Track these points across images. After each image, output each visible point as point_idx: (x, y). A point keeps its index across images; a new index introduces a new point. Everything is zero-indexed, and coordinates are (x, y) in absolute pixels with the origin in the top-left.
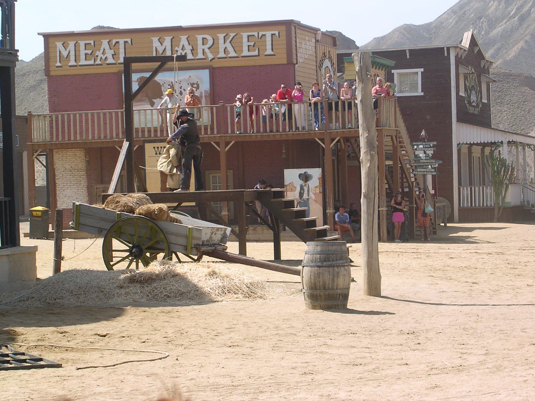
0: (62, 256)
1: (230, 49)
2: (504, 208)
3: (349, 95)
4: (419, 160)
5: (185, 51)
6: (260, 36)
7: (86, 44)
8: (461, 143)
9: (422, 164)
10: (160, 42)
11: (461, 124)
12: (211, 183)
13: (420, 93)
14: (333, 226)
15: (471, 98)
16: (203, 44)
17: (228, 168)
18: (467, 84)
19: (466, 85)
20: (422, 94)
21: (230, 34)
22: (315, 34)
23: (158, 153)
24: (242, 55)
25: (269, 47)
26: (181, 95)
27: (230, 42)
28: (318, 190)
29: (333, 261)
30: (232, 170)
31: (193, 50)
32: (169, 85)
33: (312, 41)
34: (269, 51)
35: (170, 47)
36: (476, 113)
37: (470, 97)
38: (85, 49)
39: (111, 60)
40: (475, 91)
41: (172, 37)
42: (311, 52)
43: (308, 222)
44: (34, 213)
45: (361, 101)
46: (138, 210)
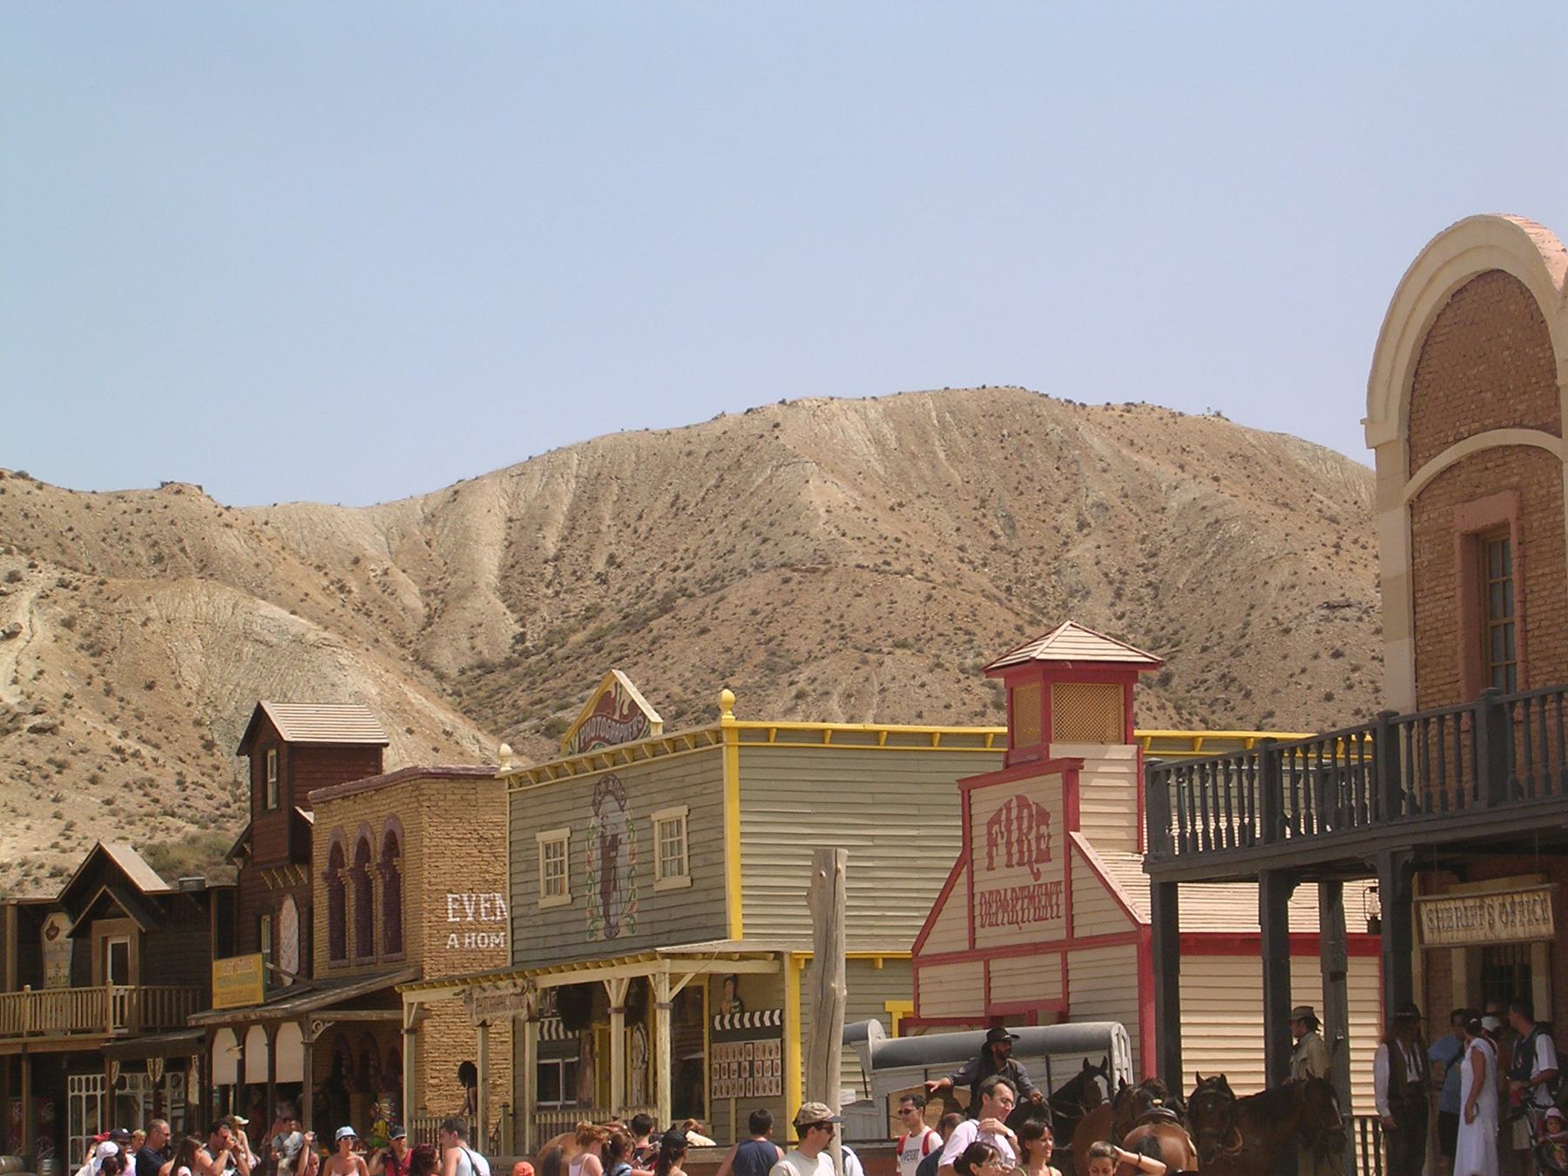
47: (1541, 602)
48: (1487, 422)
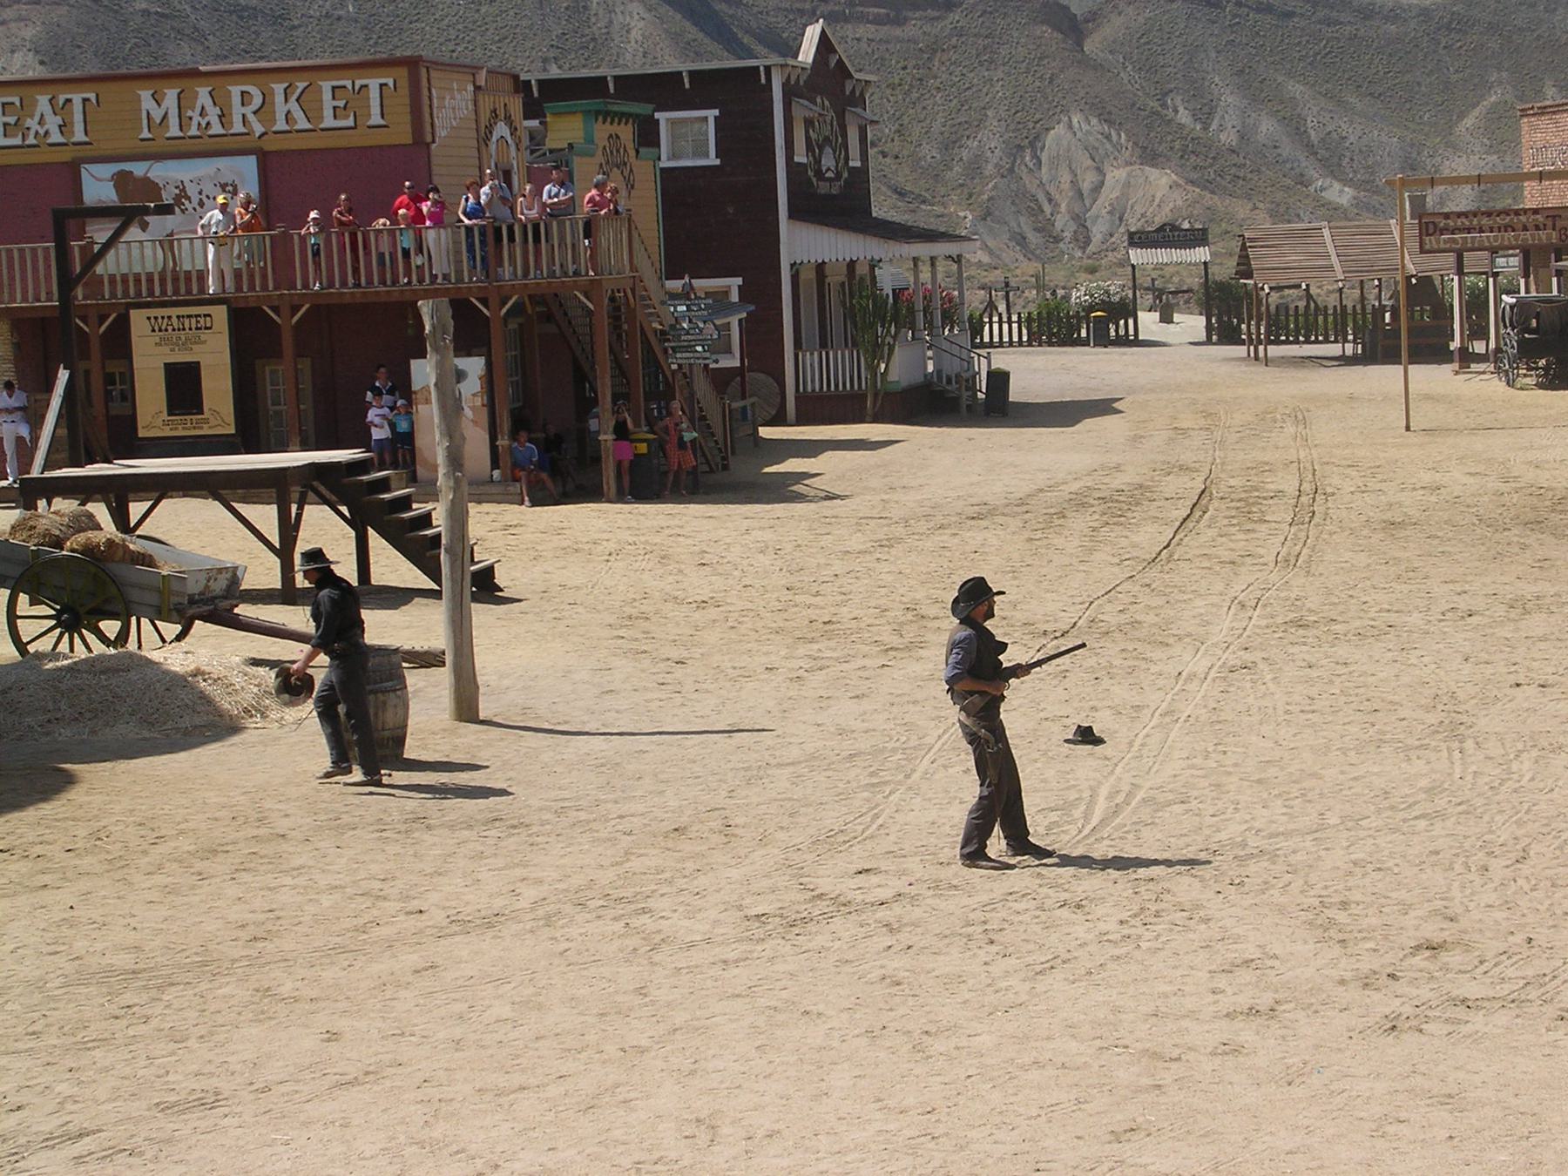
1: (298, 114)
2: (887, 394)
3: (535, 211)
4: (680, 335)
5: (207, 119)
6: (357, 88)
8: (798, 262)
9: (686, 344)
10: (157, 101)
11: (798, 223)
12: (268, 384)
13: (713, 160)
14: (509, 472)
15: (823, 162)
16: (243, 104)
17: (299, 355)
18: (813, 135)
19: (810, 138)
20: (718, 162)
21: (298, 84)
22: (474, 75)
23: (156, 328)
24: (322, 126)
25: (375, 109)
26: (202, 207)
27: (297, 100)
28: (478, 401)
29: (376, 683)
30: (309, 359)
31: (223, 115)
32: (177, 187)
33: (466, 91)
34: (376, 119)
35: (177, 110)
36: (835, 192)
37: (820, 161)
39: (56, 137)
40: (831, 146)
41: (179, 90)
42: (465, 112)
43: (412, 519)
45: (436, 385)
46: (68, 544)
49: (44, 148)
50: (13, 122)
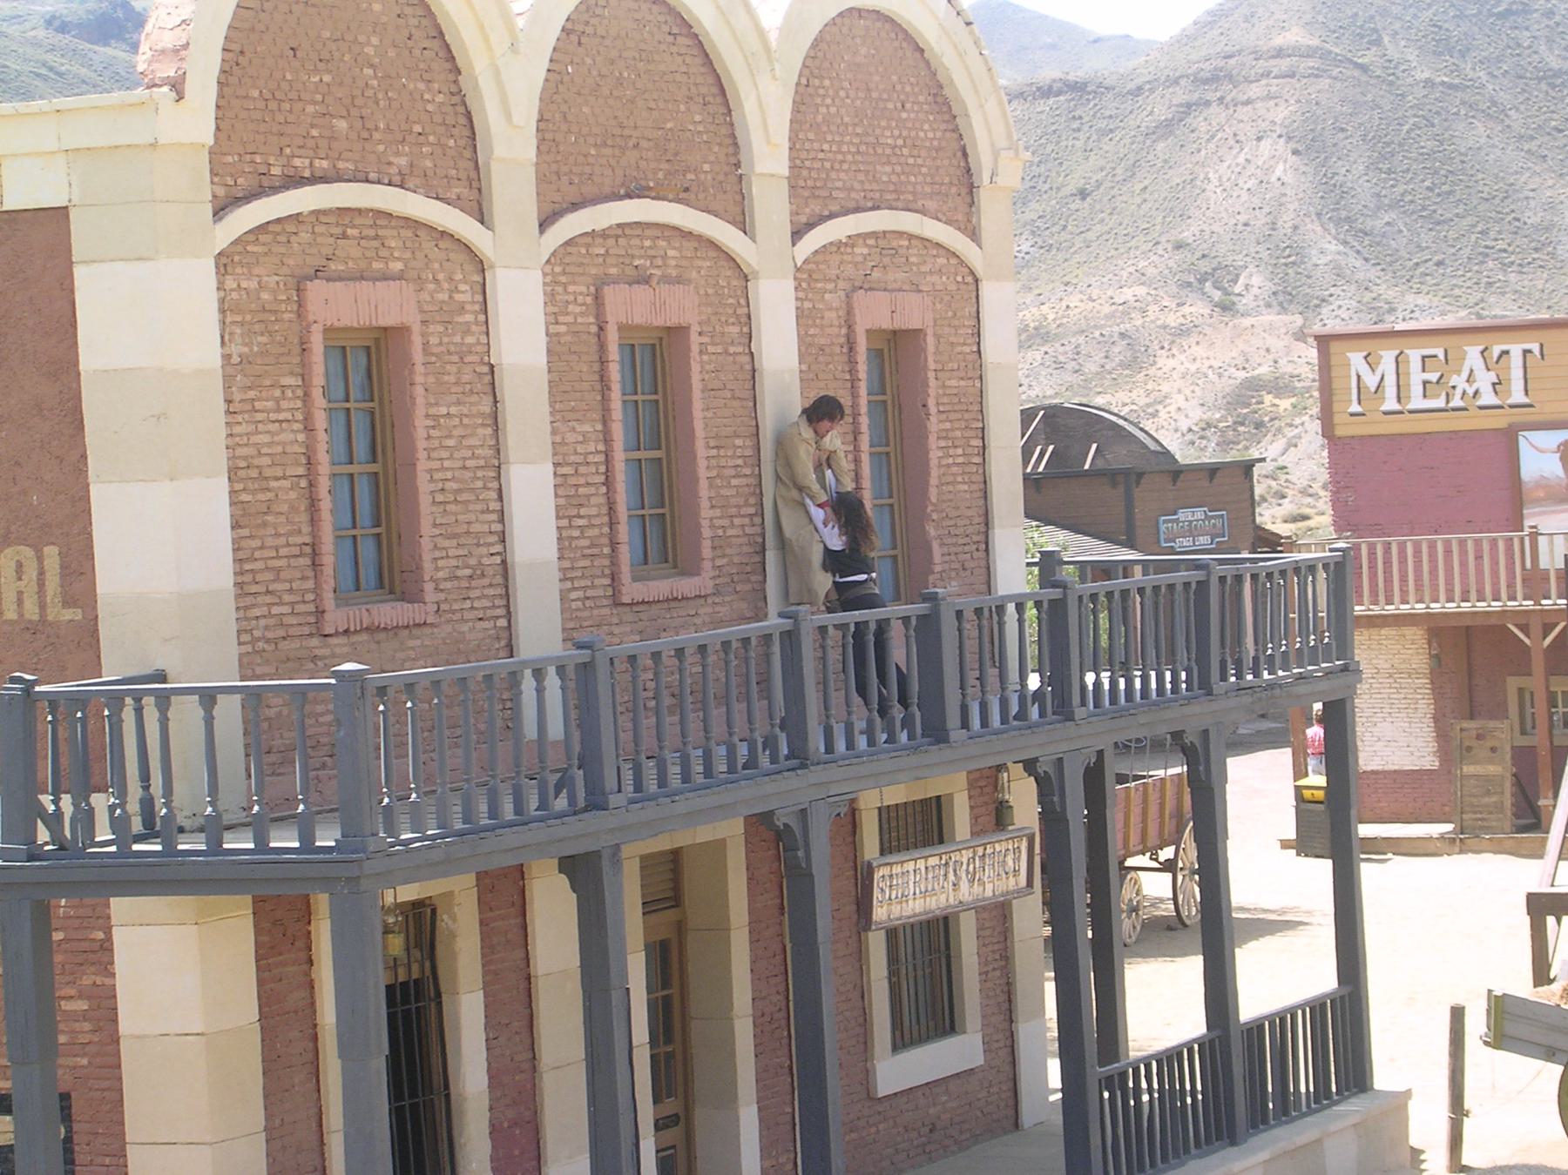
0: (1466, 1106)
7: (1424, 357)
38: (1424, 371)
39: (1488, 398)
44: (1307, 794)
47: (444, 454)
48: (341, 165)
49: (1473, 411)
50: (1435, 380)
